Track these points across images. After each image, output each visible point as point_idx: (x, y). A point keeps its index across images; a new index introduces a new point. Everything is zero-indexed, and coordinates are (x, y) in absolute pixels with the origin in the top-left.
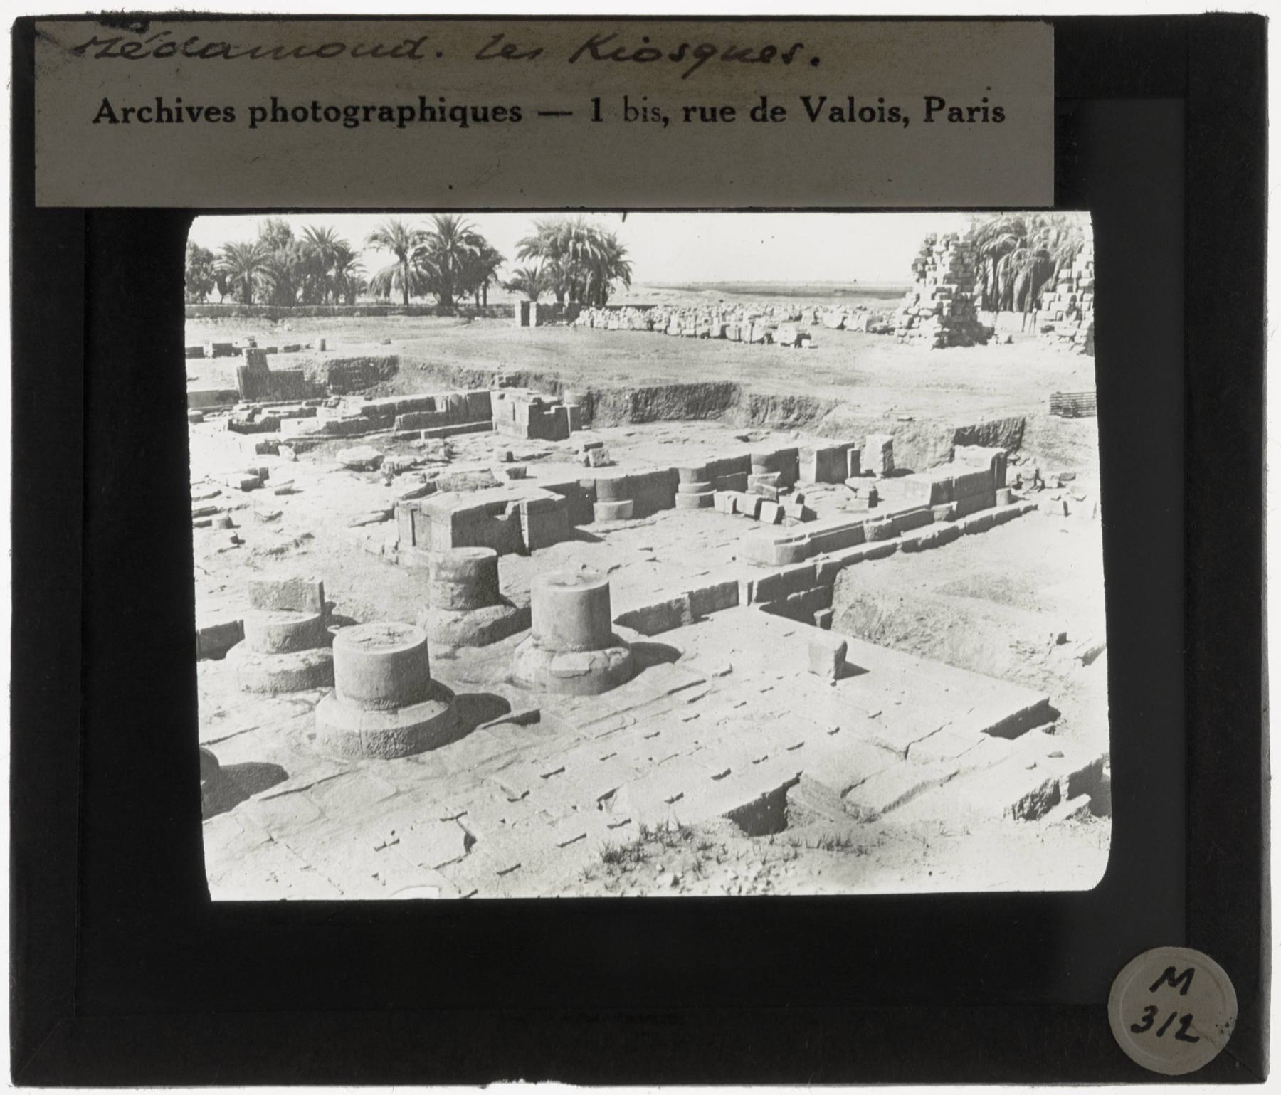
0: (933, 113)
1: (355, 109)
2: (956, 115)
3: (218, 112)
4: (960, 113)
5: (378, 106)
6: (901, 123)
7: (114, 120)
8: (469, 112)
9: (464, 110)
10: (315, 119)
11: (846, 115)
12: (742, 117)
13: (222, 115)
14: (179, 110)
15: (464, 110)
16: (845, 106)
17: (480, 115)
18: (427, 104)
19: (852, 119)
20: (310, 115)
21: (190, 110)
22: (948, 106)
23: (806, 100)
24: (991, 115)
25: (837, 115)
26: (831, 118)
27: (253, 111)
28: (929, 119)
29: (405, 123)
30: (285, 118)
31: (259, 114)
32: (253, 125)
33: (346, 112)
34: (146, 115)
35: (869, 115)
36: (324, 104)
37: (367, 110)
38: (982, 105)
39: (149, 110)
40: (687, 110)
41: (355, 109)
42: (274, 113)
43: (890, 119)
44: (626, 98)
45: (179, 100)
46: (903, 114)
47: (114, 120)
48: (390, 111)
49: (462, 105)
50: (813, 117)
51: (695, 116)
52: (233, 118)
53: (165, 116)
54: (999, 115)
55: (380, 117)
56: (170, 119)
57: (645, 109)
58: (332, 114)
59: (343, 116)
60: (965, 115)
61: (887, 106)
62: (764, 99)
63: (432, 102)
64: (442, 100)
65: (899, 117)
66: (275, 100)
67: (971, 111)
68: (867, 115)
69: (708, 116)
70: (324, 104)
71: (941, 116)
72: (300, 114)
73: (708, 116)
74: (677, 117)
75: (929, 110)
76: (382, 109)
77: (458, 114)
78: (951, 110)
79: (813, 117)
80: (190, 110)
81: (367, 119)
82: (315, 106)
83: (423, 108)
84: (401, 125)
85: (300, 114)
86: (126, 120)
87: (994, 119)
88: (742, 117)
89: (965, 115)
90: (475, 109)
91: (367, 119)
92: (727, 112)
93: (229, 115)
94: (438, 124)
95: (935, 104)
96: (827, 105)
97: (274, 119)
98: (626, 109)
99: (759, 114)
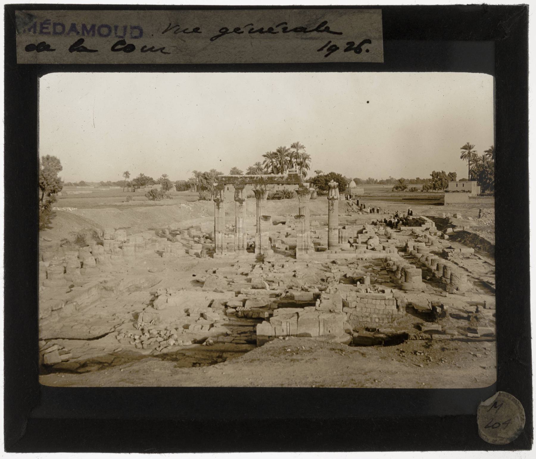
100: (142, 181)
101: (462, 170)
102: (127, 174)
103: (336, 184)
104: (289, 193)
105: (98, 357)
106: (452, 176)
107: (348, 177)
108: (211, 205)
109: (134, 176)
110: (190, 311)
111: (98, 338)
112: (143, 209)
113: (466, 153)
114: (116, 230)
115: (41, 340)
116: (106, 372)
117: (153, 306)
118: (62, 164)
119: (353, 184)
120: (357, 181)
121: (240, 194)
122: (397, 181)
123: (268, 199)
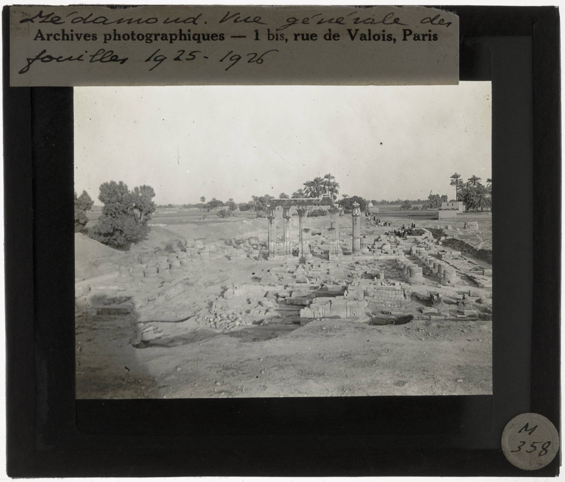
0: (407, 37)
1: (151, 35)
2: (417, 38)
3: (89, 36)
4: (418, 36)
5: (161, 33)
6: (392, 41)
7: (43, 39)
8: (201, 37)
9: (199, 35)
10: (133, 39)
11: (367, 38)
12: (320, 38)
13: (91, 37)
14: (72, 35)
15: (199, 35)
16: (367, 33)
17: (206, 37)
18: (183, 32)
19: (370, 39)
20: (131, 37)
21: (77, 35)
22: (413, 34)
23: (349, 31)
24: (432, 38)
25: (363, 37)
26: (361, 39)
27: (105, 35)
28: (405, 39)
29: (173, 41)
30: (119, 39)
31: (108, 37)
32: (105, 42)
33: (147, 35)
34: (57, 37)
35: (376, 37)
36: (136, 33)
37: (156, 36)
38: (428, 33)
39: (59, 35)
40: (296, 36)
41: (151, 35)
42: (115, 36)
43: (388, 40)
44: (269, 30)
45: (72, 31)
46: (393, 37)
47: (43, 39)
48: (166, 35)
49: (198, 33)
50: (353, 38)
51: (299, 38)
52: (96, 38)
53: (65, 37)
54: (435, 38)
55: (162, 39)
56: (68, 39)
57: (277, 35)
58: (141, 37)
59: (145, 38)
60: (421, 38)
61: (386, 34)
62: (330, 30)
63: (185, 31)
64: (189, 31)
65: (391, 39)
66: (115, 30)
67: (424, 36)
68: (376, 38)
69: (305, 37)
70: (136, 33)
71: (410, 38)
72: (126, 37)
73: (305, 37)
74: (291, 38)
75: (405, 35)
76: (162, 35)
77: (196, 37)
78: (415, 35)
79: (353, 38)
80: (77, 35)
81: (156, 39)
82: (133, 34)
83: (181, 34)
84: (171, 42)
85: (126, 37)
86: (48, 39)
87: (434, 39)
88: (320, 38)
89: (421, 38)
90: (203, 35)
91: (156, 39)
92: (313, 37)
93: (95, 37)
94: (188, 41)
95: (408, 32)
96: (359, 33)
97: (115, 39)
98: (269, 35)
99: (328, 37)
100: (215, 204)
101: (452, 193)
102: (203, 199)
103: (358, 204)
104: (323, 212)
105: (183, 335)
106: (445, 198)
107: (367, 199)
108: (265, 221)
109: (208, 200)
110: (251, 300)
111: (182, 321)
112: (215, 225)
113: (455, 181)
114: (195, 240)
115: (141, 322)
116: (189, 346)
117: (223, 297)
118: (155, 191)
119: (371, 205)
120: (374, 202)
121: (287, 213)
122: (403, 202)
123: (308, 216)
